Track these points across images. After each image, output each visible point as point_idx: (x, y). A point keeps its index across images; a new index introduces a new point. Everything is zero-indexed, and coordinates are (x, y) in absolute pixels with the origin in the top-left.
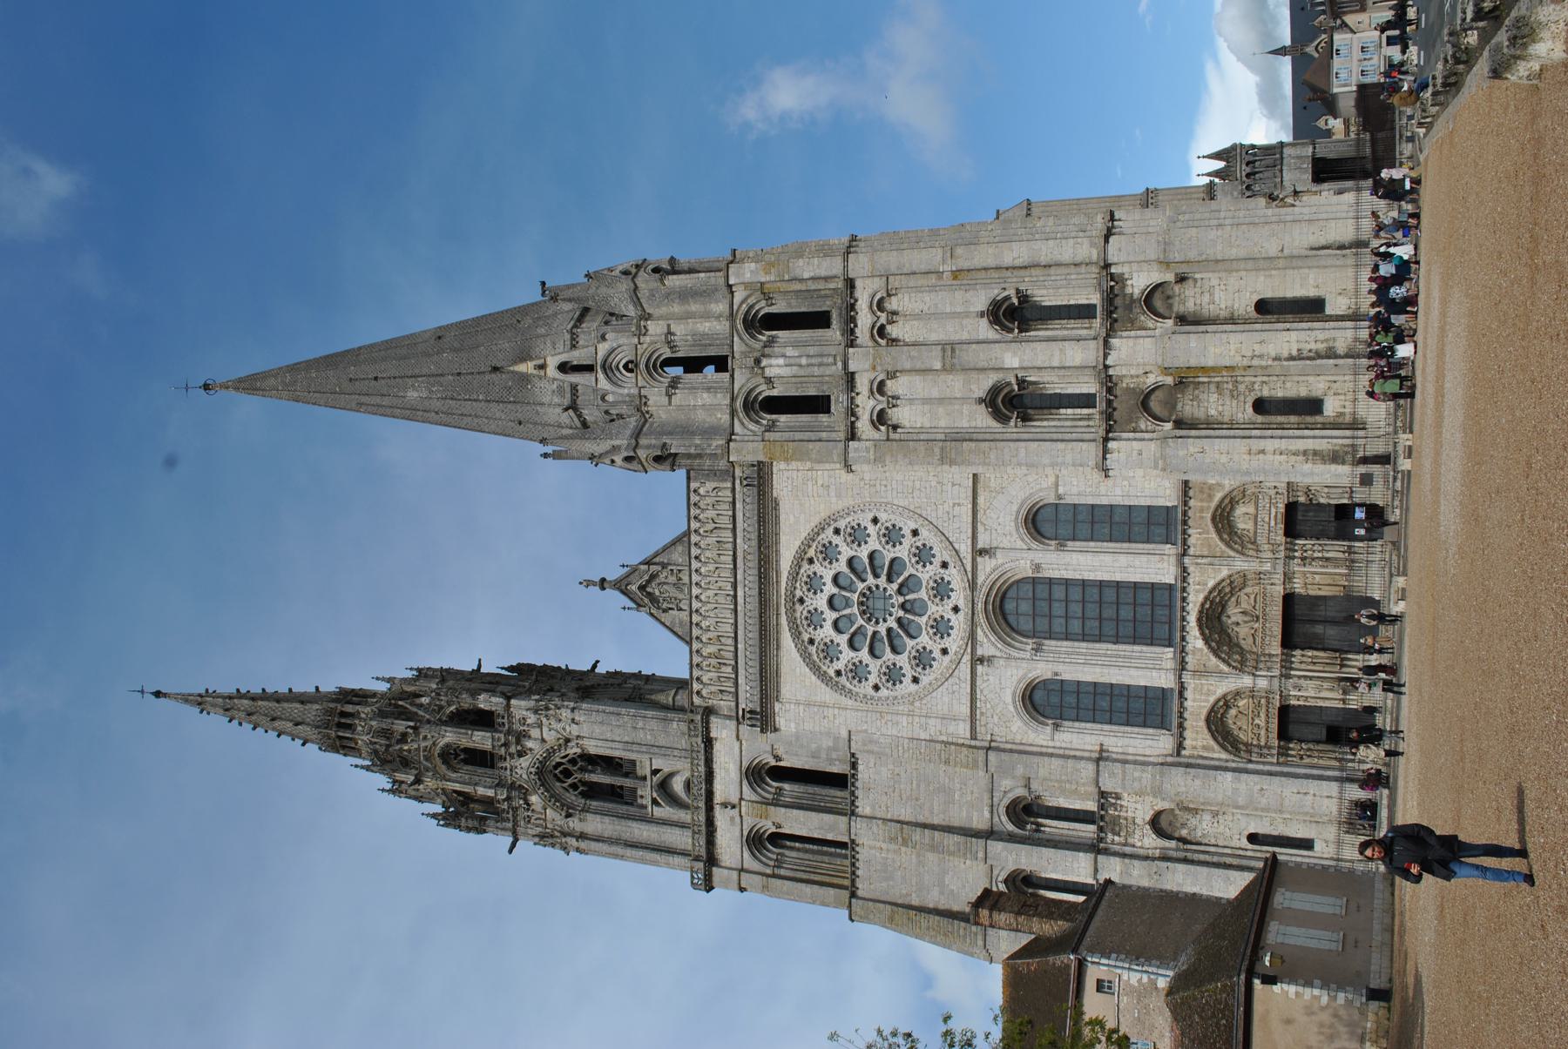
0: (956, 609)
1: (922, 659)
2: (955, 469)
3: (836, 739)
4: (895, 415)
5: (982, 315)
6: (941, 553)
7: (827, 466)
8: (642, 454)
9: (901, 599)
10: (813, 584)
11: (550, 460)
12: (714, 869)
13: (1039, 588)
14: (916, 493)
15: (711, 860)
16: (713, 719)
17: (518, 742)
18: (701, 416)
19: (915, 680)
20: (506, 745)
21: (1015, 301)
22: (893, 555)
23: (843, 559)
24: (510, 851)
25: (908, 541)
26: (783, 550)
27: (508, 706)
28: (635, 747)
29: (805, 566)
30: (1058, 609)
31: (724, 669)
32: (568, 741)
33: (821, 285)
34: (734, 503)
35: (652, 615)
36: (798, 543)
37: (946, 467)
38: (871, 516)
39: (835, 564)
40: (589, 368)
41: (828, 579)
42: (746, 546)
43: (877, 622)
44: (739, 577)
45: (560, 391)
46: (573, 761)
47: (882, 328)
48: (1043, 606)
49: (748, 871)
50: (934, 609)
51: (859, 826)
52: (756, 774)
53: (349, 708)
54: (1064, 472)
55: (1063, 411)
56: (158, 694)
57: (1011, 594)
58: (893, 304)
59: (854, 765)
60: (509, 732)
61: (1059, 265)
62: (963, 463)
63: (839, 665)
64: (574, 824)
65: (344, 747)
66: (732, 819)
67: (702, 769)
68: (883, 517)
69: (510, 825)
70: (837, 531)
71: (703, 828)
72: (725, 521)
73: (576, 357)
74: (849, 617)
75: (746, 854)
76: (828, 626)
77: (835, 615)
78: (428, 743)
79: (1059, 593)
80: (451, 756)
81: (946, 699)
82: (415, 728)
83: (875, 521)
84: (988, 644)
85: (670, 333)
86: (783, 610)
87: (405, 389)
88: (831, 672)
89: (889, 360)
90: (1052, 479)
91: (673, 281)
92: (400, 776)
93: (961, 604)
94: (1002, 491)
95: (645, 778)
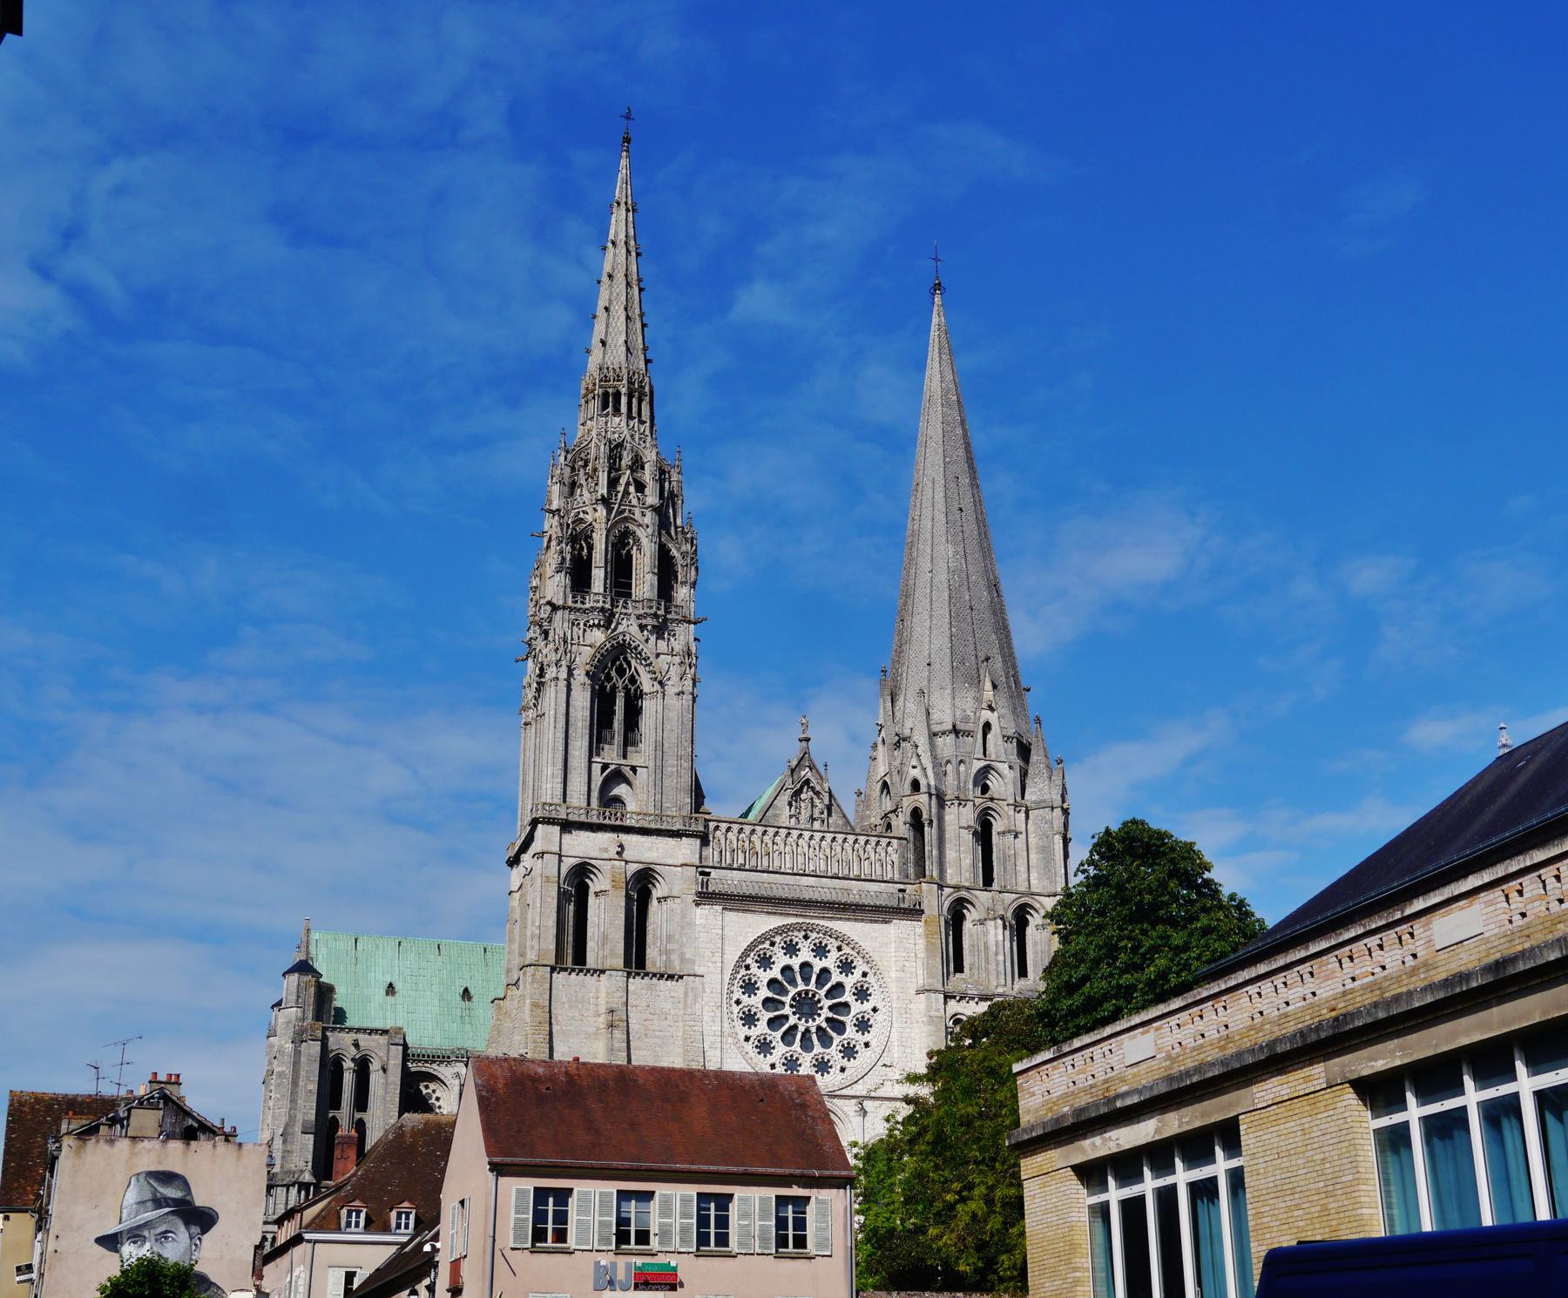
3: (694, 962)
7: (920, 972)
9: (813, 1030)
10: (820, 951)
15: (567, 826)
18: (950, 854)
31: (741, 855)
32: (661, 683)
35: (782, 789)
41: (825, 963)
45: (966, 719)
46: (633, 680)
49: (560, 861)
51: (620, 977)
60: (666, 620)
63: (754, 969)
64: (580, 677)
65: (606, 395)
66: (606, 850)
68: (879, 1016)
69: (570, 603)
75: (574, 861)
77: (796, 968)
78: (637, 516)
83: (875, 1010)
86: (800, 920)
87: (955, 544)
88: (749, 961)
91: (1058, 840)
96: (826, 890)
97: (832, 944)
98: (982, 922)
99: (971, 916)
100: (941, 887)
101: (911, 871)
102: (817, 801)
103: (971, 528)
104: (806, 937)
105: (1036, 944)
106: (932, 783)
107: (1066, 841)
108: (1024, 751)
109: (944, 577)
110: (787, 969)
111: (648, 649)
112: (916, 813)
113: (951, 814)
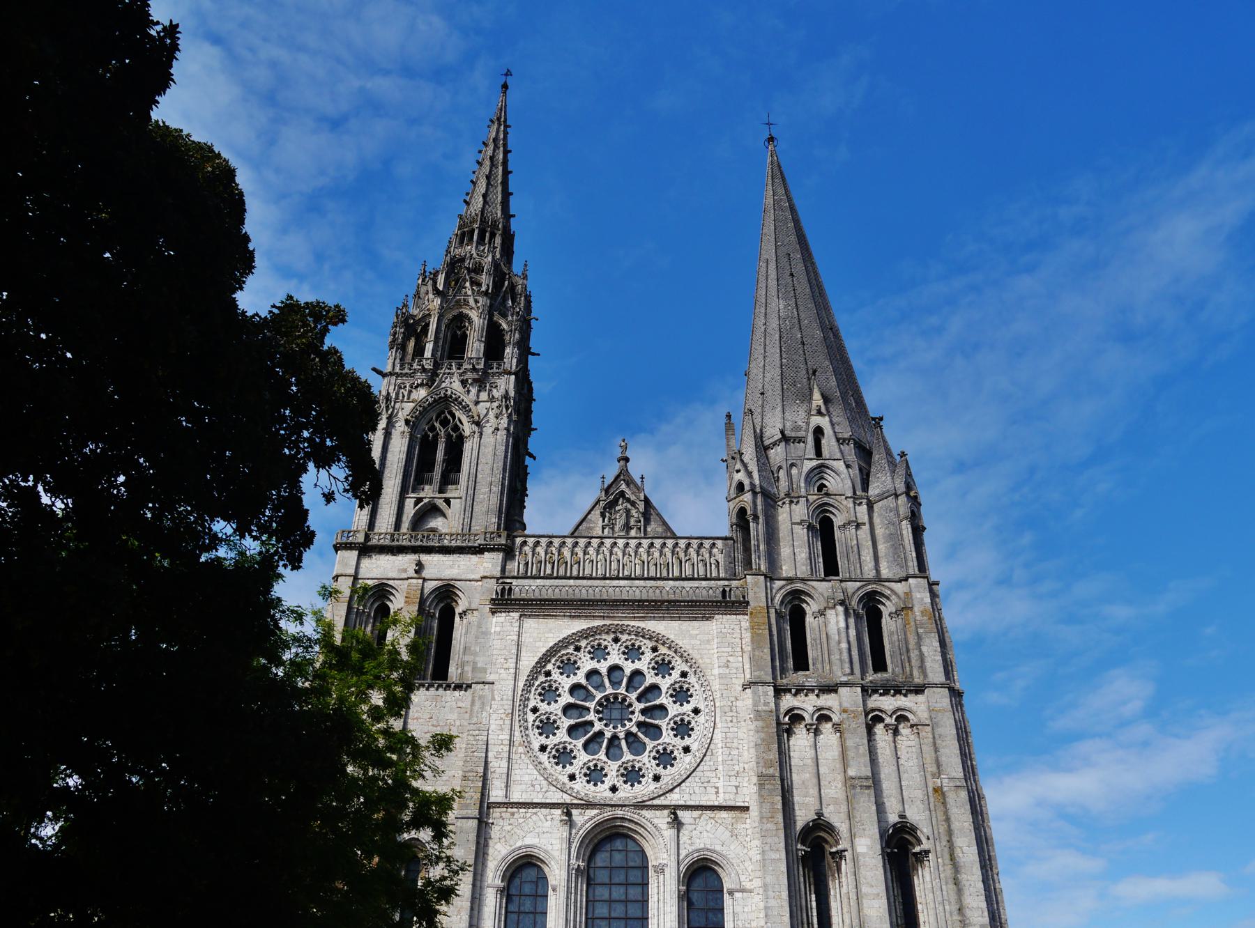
0: (614, 789)
1: (563, 756)
2: (754, 789)
3: (484, 670)
4: (800, 730)
5: (902, 816)
6: (670, 775)
7: (747, 666)
8: (747, 497)
9: (622, 735)
10: (632, 652)
11: (725, 420)
12: (356, 553)
13: (639, 873)
16: (499, 557)
17: (475, 380)
18: (785, 551)
19: (543, 748)
20: (474, 369)
21: (917, 849)
22: (664, 728)
23: (657, 680)
24: (374, 369)
25: (679, 743)
27: (510, 373)
28: (471, 484)
29: (650, 644)
30: (618, 893)
31: (549, 566)
32: (478, 424)
33: (915, 662)
34: (706, 579)
35: (598, 502)
36: (672, 637)
37: (755, 780)
39: (653, 672)
40: (819, 453)
41: (638, 665)
42: (669, 589)
43: (598, 712)
44: (637, 583)
45: (797, 428)
46: (456, 428)
47: (882, 720)
48: (620, 877)
50: (612, 768)
52: (446, 594)
53: (498, 240)
54: (757, 898)
55: (813, 896)
56: (505, 87)
57: (630, 843)
58: (904, 730)
59: (458, 687)
61: (960, 892)
62: (761, 796)
63: (556, 675)
65: (463, 234)
66: (405, 571)
67: (453, 544)
68: (701, 718)
69: (397, 370)
70: (684, 675)
71: (396, 543)
72: (688, 571)
73: (828, 443)
74: (600, 687)
76: (593, 665)
77: (604, 671)
78: (472, 302)
79: (634, 893)
80: (460, 321)
81: (526, 778)
82: (486, 293)
83: (696, 711)
84: (584, 819)
85: (858, 526)
86: (608, 622)
87: (786, 299)
89: (853, 725)
90: (748, 886)
92: (441, 279)
93: (620, 794)
94: (734, 835)
95: (440, 492)
96: (636, 590)
97: (647, 645)
98: (822, 613)
99: (811, 608)
100: (770, 577)
101: (739, 569)
102: (634, 512)
103: (803, 287)
105: (891, 634)
106: (757, 482)
107: (918, 531)
108: (865, 453)
109: (774, 323)
110: (592, 674)
111: (468, 399)
112: (742, 512)
113: (783, 515)
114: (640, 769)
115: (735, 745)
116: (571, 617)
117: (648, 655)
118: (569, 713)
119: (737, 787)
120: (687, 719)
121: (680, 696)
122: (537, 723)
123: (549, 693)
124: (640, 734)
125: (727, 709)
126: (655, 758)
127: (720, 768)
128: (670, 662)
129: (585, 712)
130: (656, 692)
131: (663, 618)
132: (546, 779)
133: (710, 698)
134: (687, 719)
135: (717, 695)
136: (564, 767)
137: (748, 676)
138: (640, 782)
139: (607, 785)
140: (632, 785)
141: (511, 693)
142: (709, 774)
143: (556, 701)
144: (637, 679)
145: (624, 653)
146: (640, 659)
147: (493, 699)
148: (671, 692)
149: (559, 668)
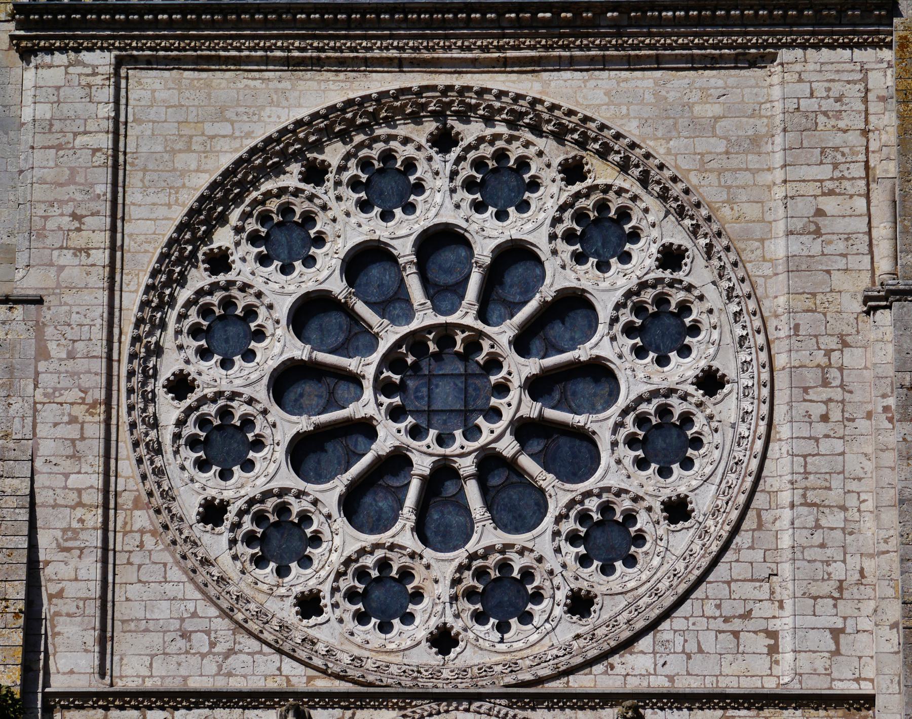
0: (443, 640)
1: (279, 537)
7: (882, 231)
9: (467, 466)
10: (498, 184)
14: (807, 516)
23: (583, 277)
26: (606, 79)
29: (557, 153)
36: (632, 130)
38: (727, 366)
39: (566, 250)
41: (517, 227)
50: (437, 571)
63: (245, 267)
68: (727, 406)
77: (405, 250)
81: (162, 611)
83: (711, 382)
86: (414, 80)
93: (465, 656)
97: (547, 156)
104: (444, 141)
110: (365, 259)
114: (527, 574)
115: (834, 497)
116: (291, 64)
117: (551, 194)
118: (291, 396)
119: (836, 633)
120: (678, 408)
121: (656, 331)
122: (191, 429)
123: (227, 329)
124: (525, 461)
125: (811, 377)
126: (573, 538)
127: (786, 569)
128: (624, 214)
129: (343, 390)
130: (579, 317)
131: (604, 64)
132: (227, 614)
133: (758, 339)
134: (678, 408)
135: (780, 329)
136: (283, 571)
137: (884, 265)
138: (526, 618)
139: (420, 630)
140: (503, 628)
141: (99, 334)
142: (747, 590)
143: (249, 356)
144: (517, 273)
145: (470, 185)
146: (524, 206)
147: (43, 353)
148: (626, 316)
149: (254, 238)
